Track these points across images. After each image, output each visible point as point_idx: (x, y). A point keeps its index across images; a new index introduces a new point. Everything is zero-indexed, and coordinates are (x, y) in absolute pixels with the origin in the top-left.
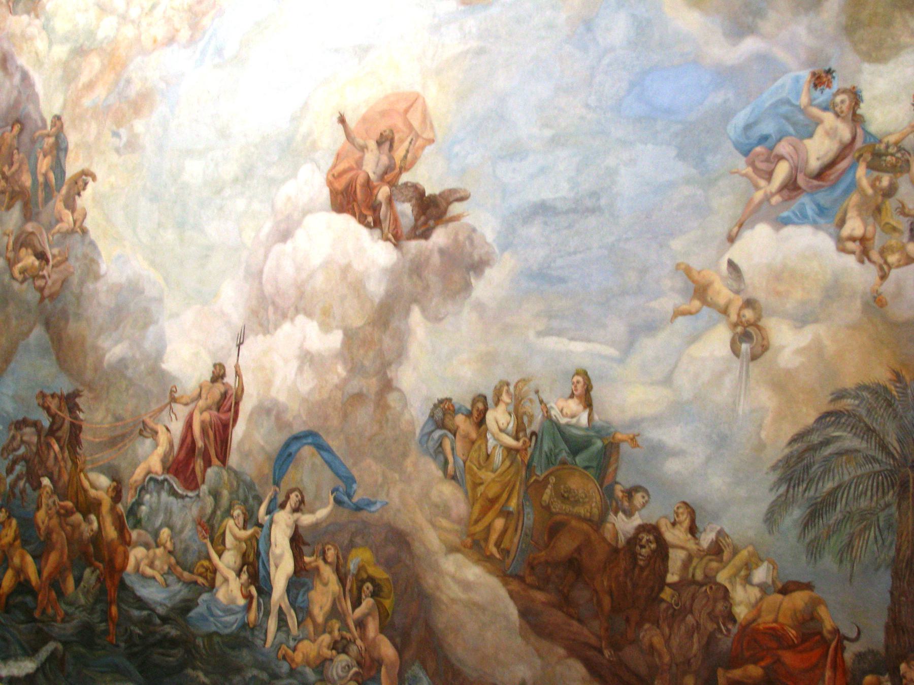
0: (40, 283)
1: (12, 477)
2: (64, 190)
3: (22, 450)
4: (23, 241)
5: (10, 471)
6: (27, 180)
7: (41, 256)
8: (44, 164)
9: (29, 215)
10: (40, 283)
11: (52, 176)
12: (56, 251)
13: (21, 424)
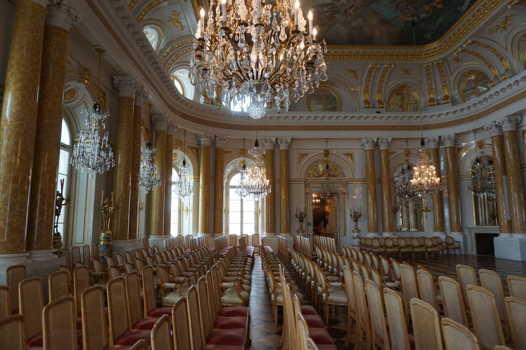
0: (359, 7)
1: (411, 9)
2: (335, 3)
3: (405, 6)
4: (345, 13)
5: (409, 9)
6: (329, 13)
7: (351, 7)
8: (326, 9)
9: (338, 12)
10: (359, 7)
11: (329, 7)
12: (351, 3)
13: (397, 7)
